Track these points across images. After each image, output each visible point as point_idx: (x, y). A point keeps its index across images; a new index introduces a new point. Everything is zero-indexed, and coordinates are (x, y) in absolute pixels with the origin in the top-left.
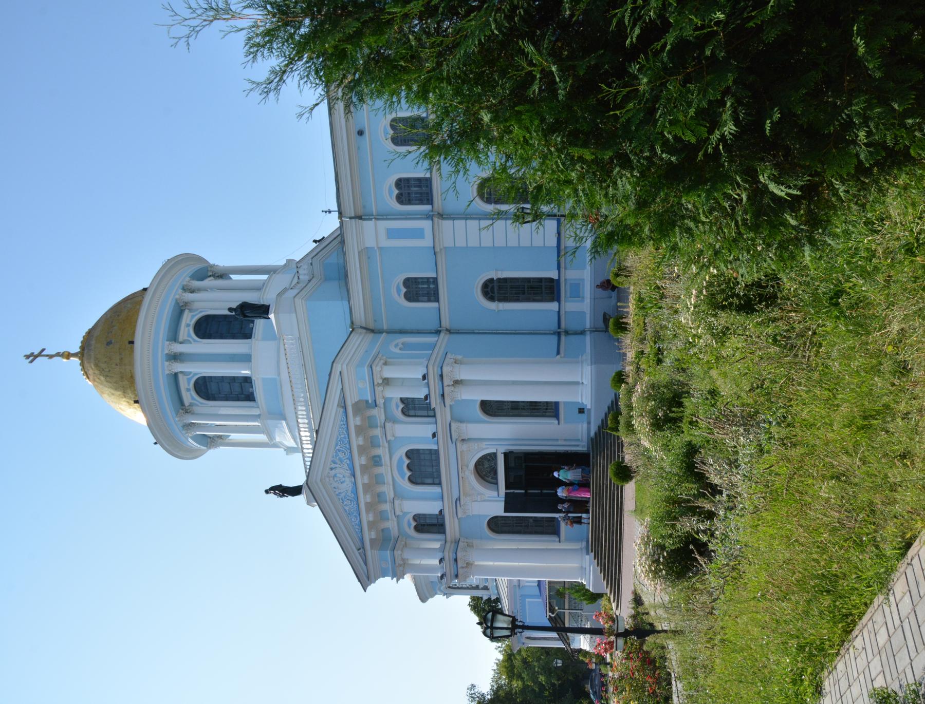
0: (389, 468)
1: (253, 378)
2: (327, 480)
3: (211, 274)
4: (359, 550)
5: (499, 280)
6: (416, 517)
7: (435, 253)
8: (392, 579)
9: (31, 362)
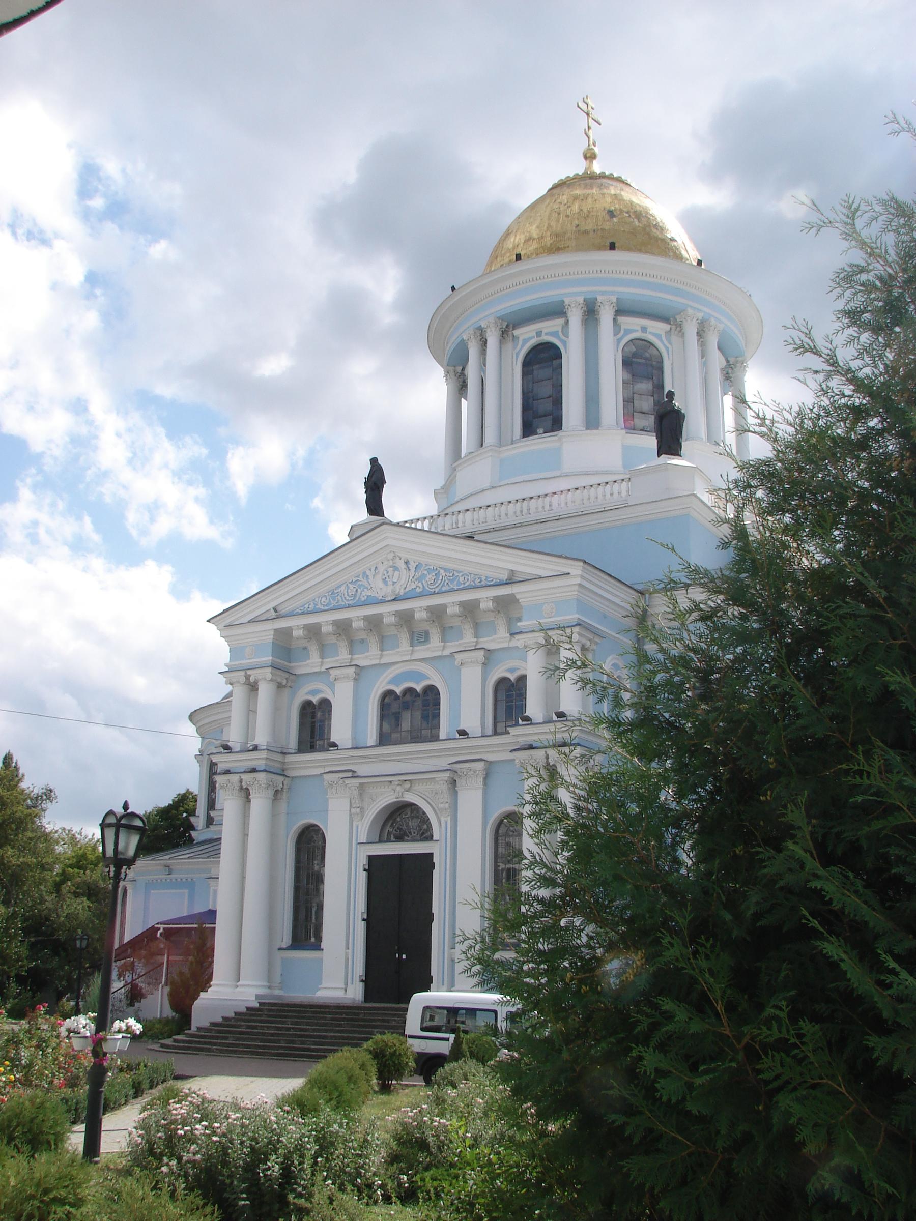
0: (408, 658)
1: (560, 433)
2: (390, 556)
4: (275, 610)
8: (226, 665)
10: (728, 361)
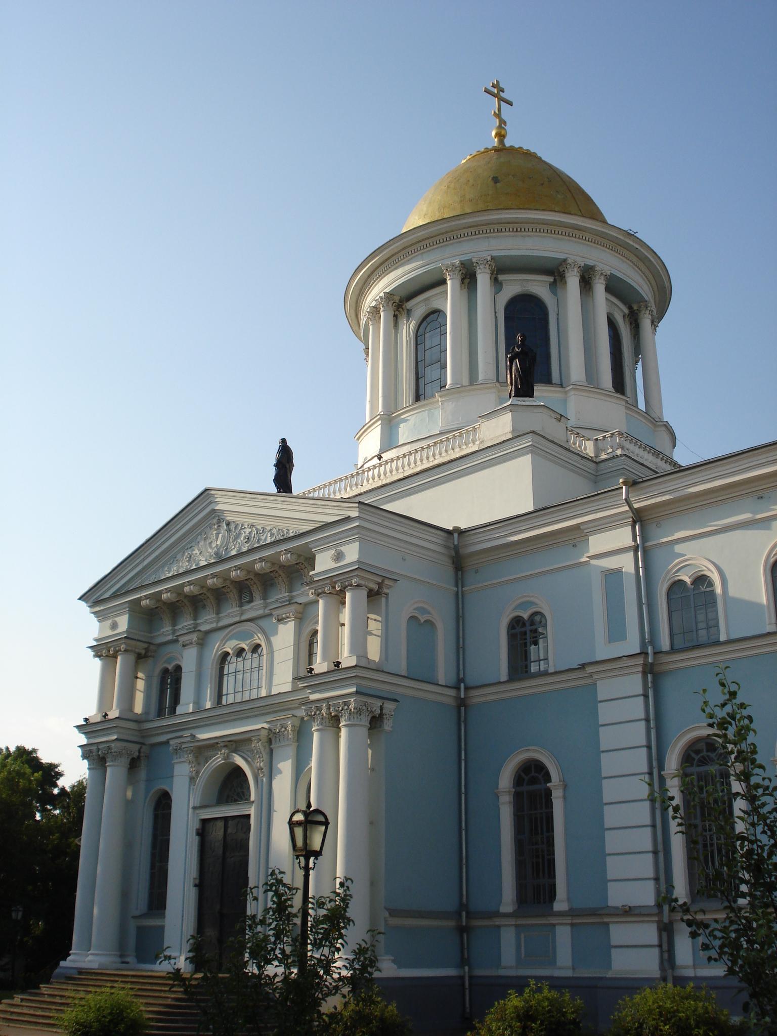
0: (237, 619)
3: (635, 308)
5: (549, 793)
6: (178, 669)
7: (583, 666)
8: (96, 640)
9: (487, 91)
10: (630, 308)
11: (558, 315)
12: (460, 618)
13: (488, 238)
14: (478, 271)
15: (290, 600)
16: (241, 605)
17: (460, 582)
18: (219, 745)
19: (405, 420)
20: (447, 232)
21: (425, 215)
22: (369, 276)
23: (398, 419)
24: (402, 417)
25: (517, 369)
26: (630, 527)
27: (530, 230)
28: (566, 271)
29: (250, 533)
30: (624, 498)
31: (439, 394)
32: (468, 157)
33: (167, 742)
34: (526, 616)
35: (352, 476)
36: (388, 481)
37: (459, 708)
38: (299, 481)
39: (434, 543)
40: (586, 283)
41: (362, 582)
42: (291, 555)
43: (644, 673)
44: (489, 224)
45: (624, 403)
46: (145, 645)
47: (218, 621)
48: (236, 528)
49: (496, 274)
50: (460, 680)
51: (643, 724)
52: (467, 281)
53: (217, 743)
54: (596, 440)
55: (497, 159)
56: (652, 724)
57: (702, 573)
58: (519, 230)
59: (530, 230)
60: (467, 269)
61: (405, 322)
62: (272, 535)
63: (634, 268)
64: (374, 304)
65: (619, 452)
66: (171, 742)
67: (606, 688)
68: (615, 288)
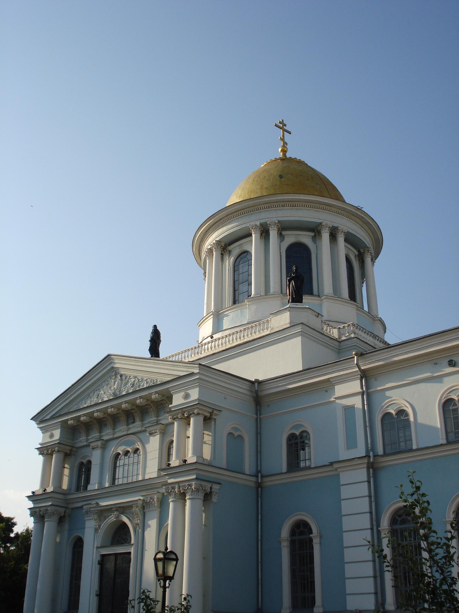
0: (125, 433)
3: (362, 251)
5: (311, 540)
6: (90, 462)
7: (331, 464)
8: (40, 444)
9: (276, 125)
10: (359, 251)
11: (317, 255)
12: (258, 434)
13: (276, 210)
14: (271, 229)
15: (157, 422)
16: (128, 425)
17: (258, 412)
18: (113, 509)
19: (227, 315)
20: (253, 206)
21: (240, 196)
22: (207, 231)
23: (223, 315)
24: (225, 313)
25: (293, 286)
26: (359, 381)
27: (301, 205)
28: (322, 230)
29: (134, 381)
30: (355, 363)
31: (247, 300)
32: (265, 163)
33: (81, 507)
34: (297, 433)
35: (195, 348)
36: (217, 351)
37: (257, 488)
38: (164, 350)
39: (244, 389)
40: (333, 237)
41: (201, 412)
42: (158, 395)
43: (368, 468)
44: (277, 202)
45: (355, 307)
46: (70, 448)
47: (114, 434)
48: (126, 378)
49: (281, 231)
50: (258, 472)
51: (367, 499)
52: (264, 234)
53: (112, 508)
54: (339, 328)
55: (282, 164)
56: (373, 499)
57: (402, 408)
58: (294, 205)
59: (301, 205)
60: (264, 227)
61: (228, 258)
62: (147, 383)
63: (361, 228)
64: (209, 247)
65: (353, 336)
66: (84, 507)
67: (345, 477)
68: (350, 239)
